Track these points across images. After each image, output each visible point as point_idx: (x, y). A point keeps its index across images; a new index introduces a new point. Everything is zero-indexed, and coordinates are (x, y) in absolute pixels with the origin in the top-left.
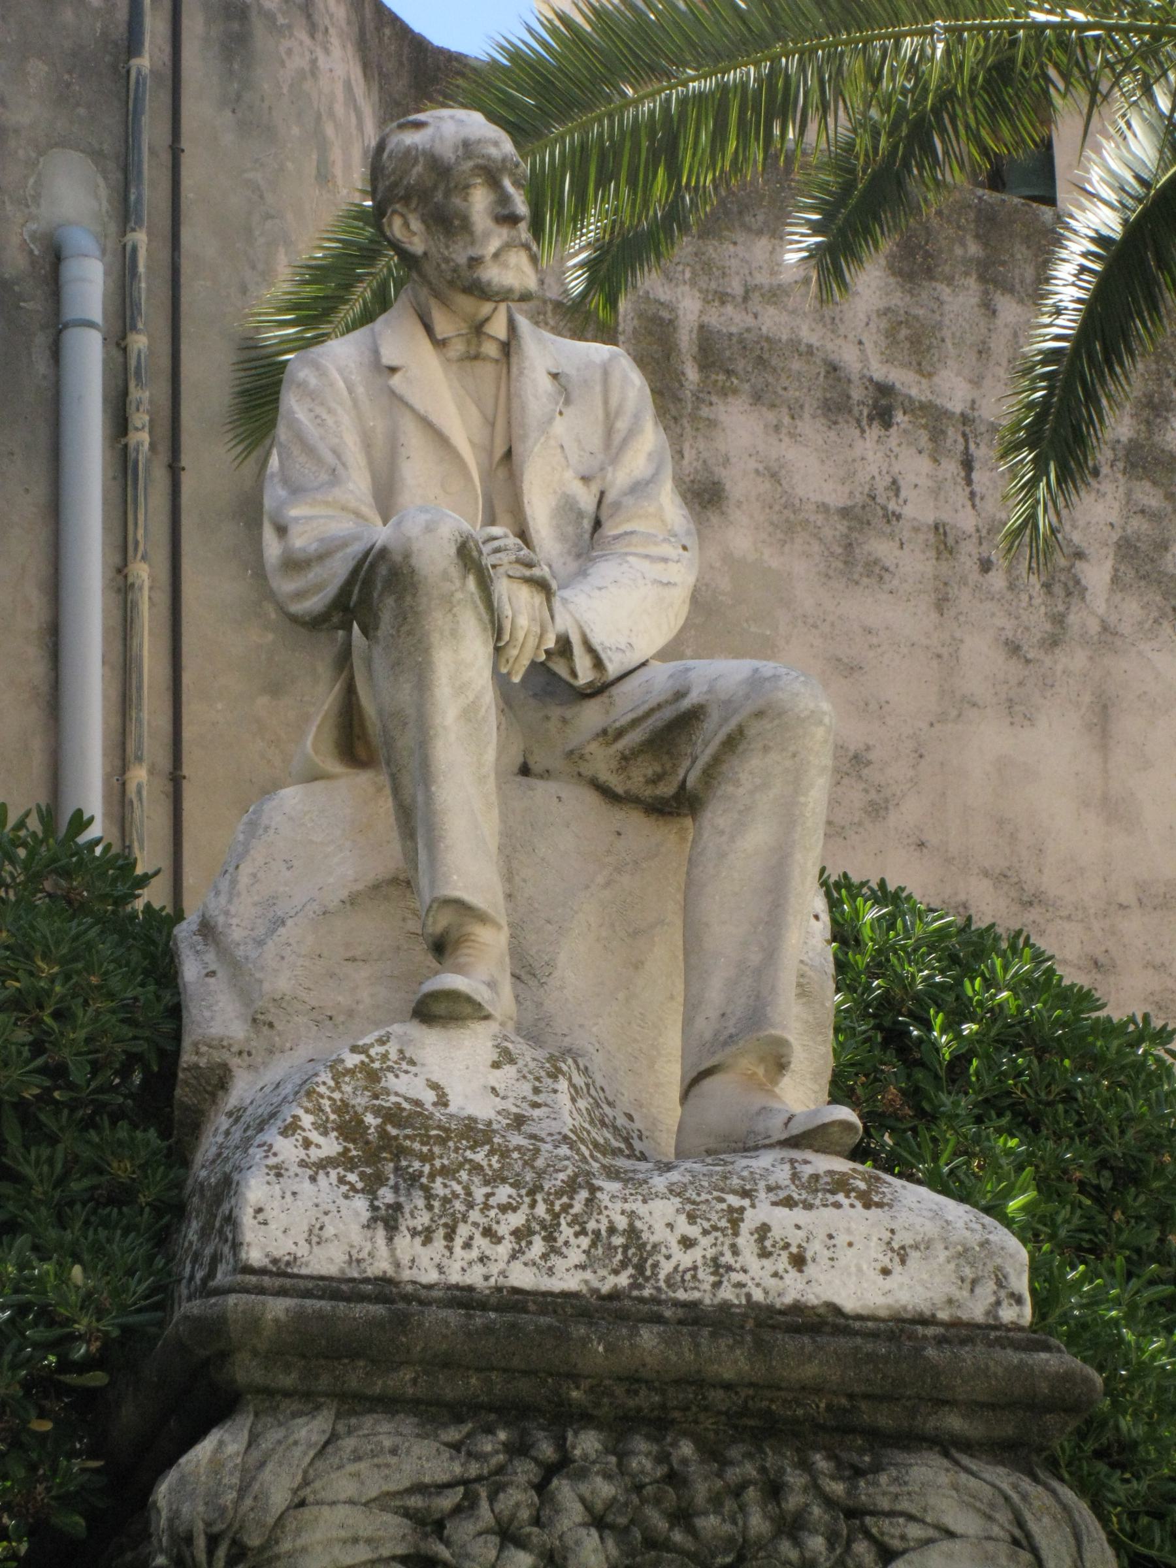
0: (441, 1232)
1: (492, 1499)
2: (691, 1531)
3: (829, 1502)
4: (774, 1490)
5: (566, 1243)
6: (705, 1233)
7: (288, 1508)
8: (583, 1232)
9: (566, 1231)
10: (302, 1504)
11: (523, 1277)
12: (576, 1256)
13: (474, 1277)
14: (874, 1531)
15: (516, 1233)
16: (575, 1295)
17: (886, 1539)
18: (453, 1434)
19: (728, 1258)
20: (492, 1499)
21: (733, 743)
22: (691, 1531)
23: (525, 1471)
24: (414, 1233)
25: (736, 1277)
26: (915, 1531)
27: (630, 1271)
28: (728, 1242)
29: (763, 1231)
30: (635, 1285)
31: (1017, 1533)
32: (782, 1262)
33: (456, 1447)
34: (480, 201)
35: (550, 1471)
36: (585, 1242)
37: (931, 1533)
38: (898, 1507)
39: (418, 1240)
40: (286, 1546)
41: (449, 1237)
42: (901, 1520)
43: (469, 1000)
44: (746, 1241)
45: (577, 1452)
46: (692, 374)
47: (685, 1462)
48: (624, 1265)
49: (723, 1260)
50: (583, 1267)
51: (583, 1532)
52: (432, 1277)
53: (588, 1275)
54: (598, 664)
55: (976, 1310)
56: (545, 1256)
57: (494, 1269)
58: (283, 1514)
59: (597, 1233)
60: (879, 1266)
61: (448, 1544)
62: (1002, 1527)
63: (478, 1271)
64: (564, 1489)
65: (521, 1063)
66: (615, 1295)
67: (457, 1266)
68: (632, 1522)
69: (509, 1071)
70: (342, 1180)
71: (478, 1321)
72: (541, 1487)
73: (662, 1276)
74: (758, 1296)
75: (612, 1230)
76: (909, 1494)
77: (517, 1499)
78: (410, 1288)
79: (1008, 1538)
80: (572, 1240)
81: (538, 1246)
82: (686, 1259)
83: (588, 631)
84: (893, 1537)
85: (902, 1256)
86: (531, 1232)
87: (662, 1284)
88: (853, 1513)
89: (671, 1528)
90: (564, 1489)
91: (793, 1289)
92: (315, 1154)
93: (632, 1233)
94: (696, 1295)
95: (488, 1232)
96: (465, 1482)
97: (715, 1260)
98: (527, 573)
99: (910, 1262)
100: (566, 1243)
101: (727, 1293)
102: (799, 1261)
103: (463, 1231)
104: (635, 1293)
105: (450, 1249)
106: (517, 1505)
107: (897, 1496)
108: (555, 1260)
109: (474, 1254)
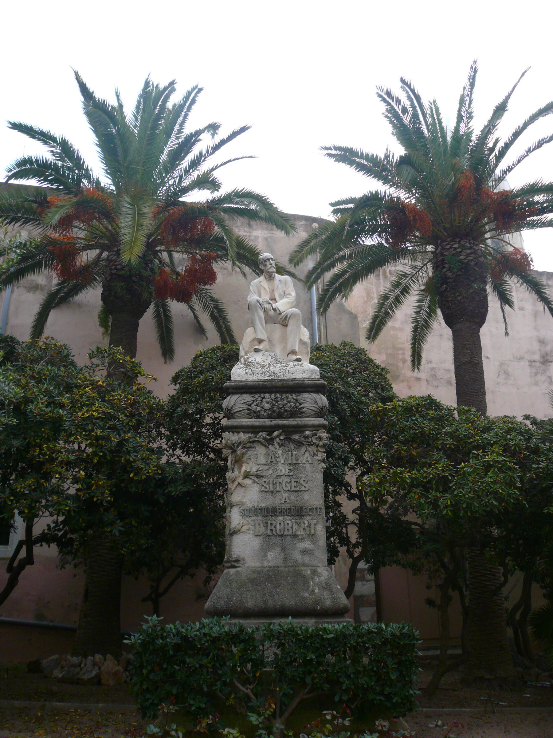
3: (294, 399)
4: (288, 398)
11: (261, 378)
13: (256, 379)
21: (289, 318)
23: (259, 399)
26: (303, 402)
32: (291, 374)
34: (268, 263)
44: (287, 372)
46: (389, 275)
64: (264, 400)
72: (261, 400)
90: (264, 400)
91: (293, 376)
93: (274, 373)
101: (284, 378)
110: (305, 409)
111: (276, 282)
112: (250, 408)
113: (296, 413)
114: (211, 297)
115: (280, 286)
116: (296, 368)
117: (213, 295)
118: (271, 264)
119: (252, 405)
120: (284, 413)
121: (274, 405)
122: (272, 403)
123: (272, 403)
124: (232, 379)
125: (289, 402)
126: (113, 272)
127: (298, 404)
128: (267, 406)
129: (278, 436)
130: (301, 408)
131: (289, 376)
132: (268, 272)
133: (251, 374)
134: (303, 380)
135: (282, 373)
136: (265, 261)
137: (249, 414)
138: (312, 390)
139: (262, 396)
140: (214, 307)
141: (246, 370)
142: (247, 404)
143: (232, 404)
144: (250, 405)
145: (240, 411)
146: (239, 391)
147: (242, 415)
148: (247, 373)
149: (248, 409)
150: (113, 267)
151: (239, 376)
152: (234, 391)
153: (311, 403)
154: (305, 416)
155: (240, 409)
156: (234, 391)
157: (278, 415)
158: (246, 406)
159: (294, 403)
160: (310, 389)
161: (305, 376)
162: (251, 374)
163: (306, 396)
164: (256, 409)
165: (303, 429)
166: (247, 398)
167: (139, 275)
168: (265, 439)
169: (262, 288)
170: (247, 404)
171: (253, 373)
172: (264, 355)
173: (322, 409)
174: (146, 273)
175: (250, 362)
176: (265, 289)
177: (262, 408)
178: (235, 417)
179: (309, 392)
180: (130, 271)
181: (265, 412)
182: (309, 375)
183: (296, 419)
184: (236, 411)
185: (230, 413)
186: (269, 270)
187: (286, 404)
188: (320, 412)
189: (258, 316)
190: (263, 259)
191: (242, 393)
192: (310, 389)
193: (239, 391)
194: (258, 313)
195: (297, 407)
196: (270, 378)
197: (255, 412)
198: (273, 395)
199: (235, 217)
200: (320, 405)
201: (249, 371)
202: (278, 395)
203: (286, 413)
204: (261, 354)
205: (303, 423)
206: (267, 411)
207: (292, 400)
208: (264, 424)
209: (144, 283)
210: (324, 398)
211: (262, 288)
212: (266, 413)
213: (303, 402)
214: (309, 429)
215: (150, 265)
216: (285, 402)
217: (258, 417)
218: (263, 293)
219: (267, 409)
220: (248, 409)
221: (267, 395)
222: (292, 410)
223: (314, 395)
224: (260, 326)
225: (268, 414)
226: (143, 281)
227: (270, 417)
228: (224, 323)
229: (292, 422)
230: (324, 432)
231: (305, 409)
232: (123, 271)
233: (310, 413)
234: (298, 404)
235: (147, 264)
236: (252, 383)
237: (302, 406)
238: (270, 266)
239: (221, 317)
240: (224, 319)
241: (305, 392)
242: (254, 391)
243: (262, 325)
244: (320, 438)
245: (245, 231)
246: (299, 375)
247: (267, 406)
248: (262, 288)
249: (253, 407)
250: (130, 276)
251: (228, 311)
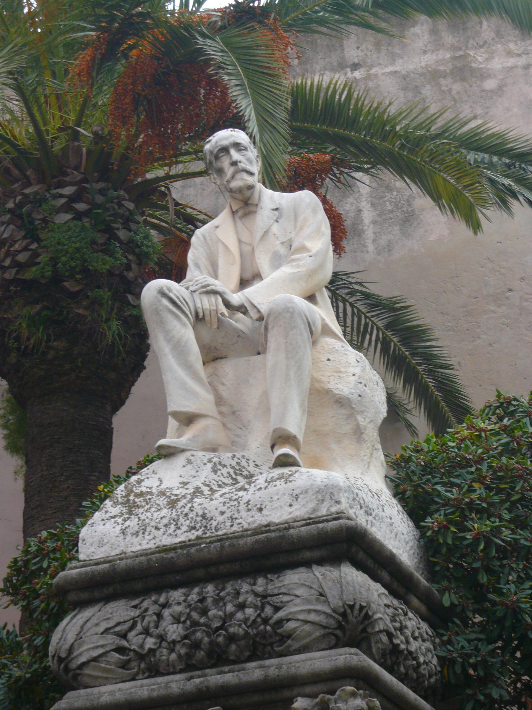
0: (142, 531)
1: (142, 622)
2: (208, 617)
3: (256, 595)
5: (182, 525)
6: (229, 508)
7: (76, 640)
8: (188, 519)
9: (182, 520)
10: (81, 638)
11: (167, 541)
12: (184, 528)
13: (152, 545)
14: (271, 602)
15: (166, 526)
16: (184, 542)
17: (276, 604)
18: (136, 602)
19: (236, 515)
20: (142, 622)
22: (208, 617)
24: (133, 534)
25: (238, 521)
26: (286, 598)
27: (203, 528)
28: (236, 509)
29: (248, 503)
30: (205, 533)
31: (321, 590)
32: (254, 512)
33: (135, 607)
35: (164, 606)
36: (188, 522)
37: (292, 598)
38: (281, 591)
39: (135, 536)
40: (75, 654)
41: (144, 533)
42: (280, 596)
43: (169, 447)
44: (243, 507)
45: (172, 599)
47: (208, 592)
48: (200, 527)
49: (234, 516)
50: (187, 531)
51: (171, 626)
52: (138, 548)
53: (189, 534)
54: (259, 311)
55: (323, 511)
56: (175, 531)
57: (157, 540)
58: (72, 645)
59: (192, 518)
60: (288, 504)
61: (128, 641)
62: (315, 590)
63: (153, 541)
64: (166, 613)
65: (194, 463)
66: (198, 538)
67: (145, 542)
68: (187, 619)
69: (190, 466)
70: (115, 522)
71: (137, 561)
73: (213, 528)
74: (246, 526)
75: (197, 515)
76: (284, 585)
77: (150, 619)
78: (132, 554)
79: (318, 594)
80: (184, 523)
81: (173, 527)
82: (220, 519)
83: (252, 300)
84: (277, 603)
85: (297, 497)
86: (170, 524)
87: (213, 531)
88: (264, 597)
89: (201, 617)
90: (166, 613)
91: (260, 519)
92: (108, 515)
93: (204, 516)
94: (224, 531)
95: (157, 528)
96: (133, 619)
97: (231, 517)
98: (204, 290)
99: (299, 500)
100: (182, 525)
101: (235, 528)
102: (260, 510)
103: (148, 529)
104: (204, 536)
105: (144, 537)
106: (149, 622)
107: (280, 587)
108: (179, 532)
109: (151, 537)
110: (291, 625)
111: (264, 216)
112: (124, 643)
113: (268, 640)
114: (367, 296)
115: (275, 228)
116: (271, 489)
117: (373, 289)
118: (234, 164)
119: (131, 635)
120: (228, 646)
121: (195, 624)
122: (189, 617)
123: (189, 617)
124: (82, 557)
125: (242, 607)
126: (7, 276)
127: (268, 610)
128: (174, 631)
130: (280, 623)
131: (249, 520)
132: (231, 191)
133: (137, 534)
134: (287, 526)
135: (228, 514)
136: (217, 157)
137: (124, 666)
138: (317, 554)
139: (162, 600)
140: (388, 327)
141: (125, 520)
142: (117, 634)
143: (71, 637)
144: (124, 636)
145: (95, 659)
146: (96, 594)
147: (105, 670)
148: (124, 532)
149: (120, 650)
150: (7, 262)
151: (101, 544)
152: (84, 596)
153: (308, 601)
154: (296, 646)
155: (95, 653)
156: (84, 596)
157: (210, 654)
158: (111, 640)
159: (256, 607)
160: (308, 555)
161: (300, 510)
162: (137, 534)
163: (293, 578)
164: (142, 646)
165: (286, 693)
166: (120, 611)
167: (85, 270)
169: (220, 247)
170: (117, 634)
171: (143, 529)
172: (189, 462)
173: (344, 615)
174: (102, 263)
175: (141, 494)
176: (226, 247)
177: (162, 638)
178: (86, 680)
179: (308, 564)
180: (54, 266)
181: (172, 650)
182: (311, 505)
183: (267, 662)
184: (83, 659)
185: (67, 669)
186: (234, 184)
187: (232, 615)
188: (340, 627)
189: (169, 339)
190: (211, 152)
191: (108, 599)
192: (308, 555)
193: (96, 594)
194: (167, 333)
195: (266, 621)
196: (193, 535)
197: (141, 657)
198: (196, 590)
199: (471, 15)
200: (335, 601)
201: (133, 523)
202: (210, 588)
203: (233, 647)
204: (181, 460)
205: (284, 671)
206: (178, 647)
207: (251, 599)
208: (163, 692)
209: (105, 294)
211: (221, 249)
212: (173, 656)
213: (286, 598)
214: (308, 689)
215: (122, 234)
216: (230, 608)
217: (154, 671)
219: (174, 642)
220: (120, 650)
221: (177, 595)
222: (251, 631)
223: (318, 571)
224: (180, 372)
225: (180, 656)
226: (99, 287)
227: (189, 666)
228: (431, 372)
229: (254, 672)
230: (354, 695)
231: (291, 625)
232: (34, 269)
233: (309, 634)
234: (268, 610)
235: (109, 231)
236: (129, 561)
237: (281, 614)
238: (232, 169)
239: (414, 355)
240: (429, 358)
241: (294, 566)
242: (139, 585)
243: (188, 367)
245: (509, 53)
247: (174, 631)
248: (221, 249)
249: (135, 640)
250: (57, 279)
251: (437, 333)
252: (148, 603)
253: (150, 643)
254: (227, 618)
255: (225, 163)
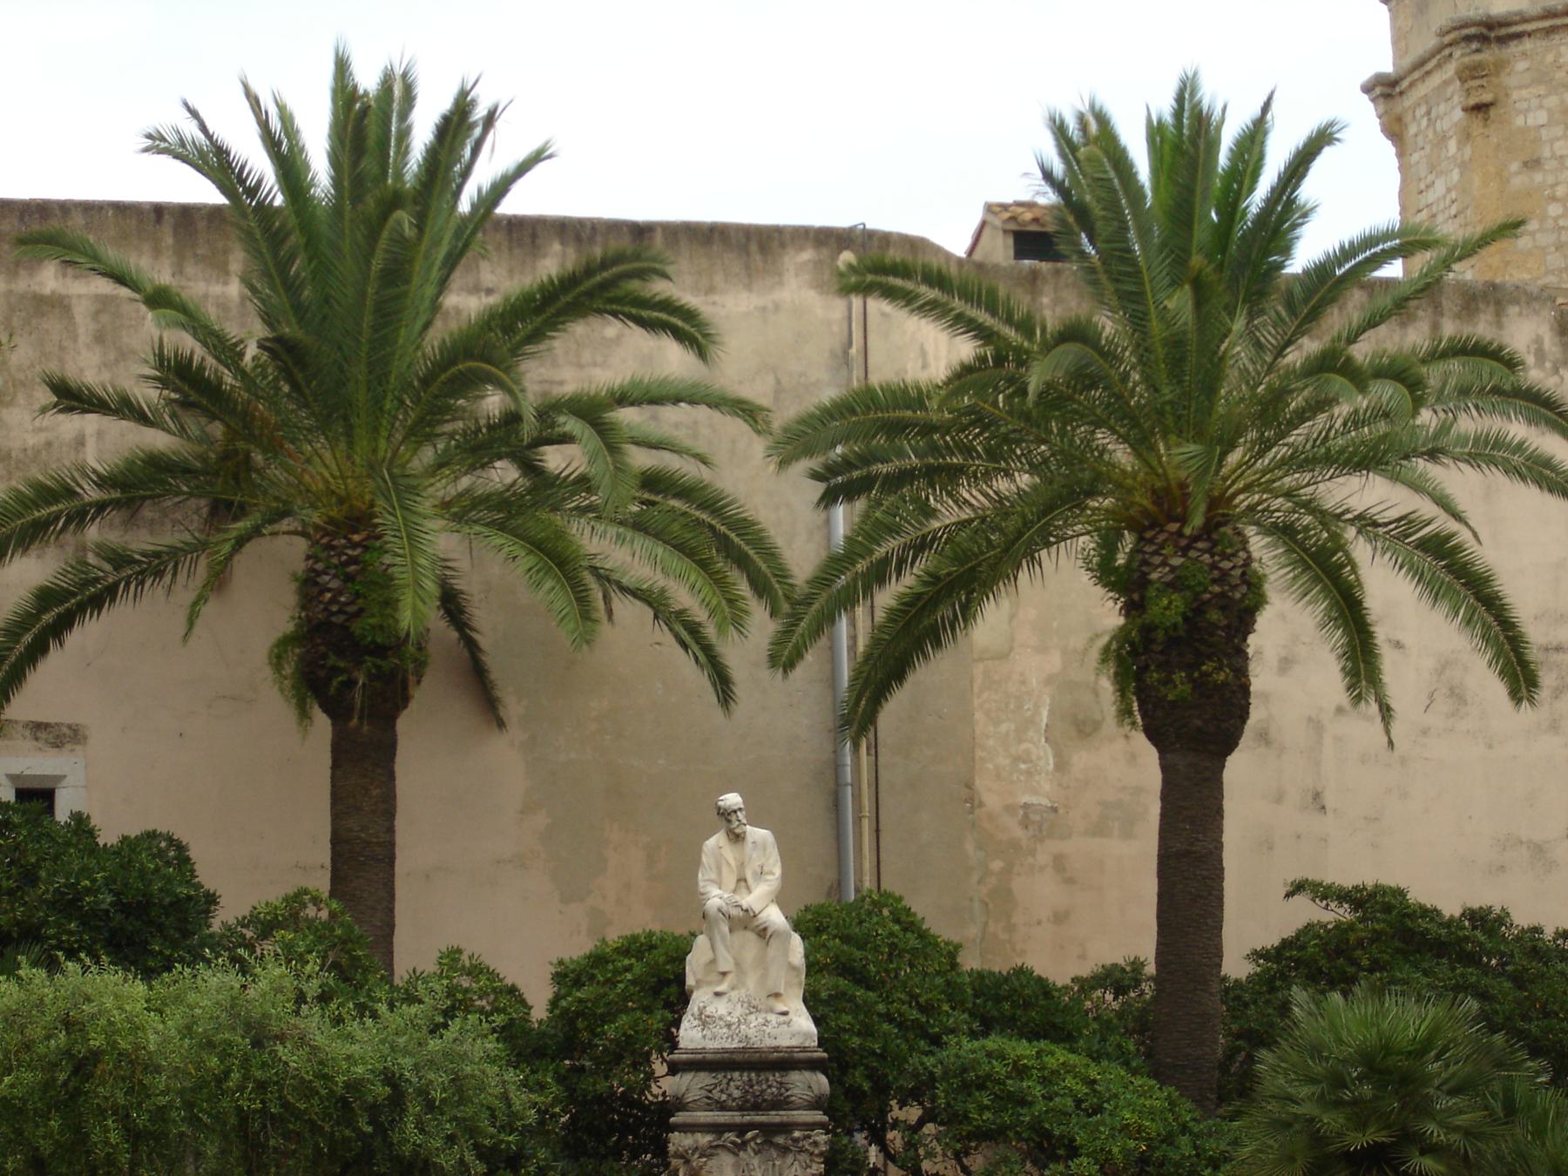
77: (724, 1086)
91: (775, 1043)
128: (737, 1093)
129: (753, 1139)
131: (769, 1043)
158: (704, 1093)
166: (704, 1079)
168: (733, 1143)
204: (725, 999)
210: (823, 1079)
218: (725, 869)
221: (736, 1075)
227: (740, 1109)
229: (775, 1117)
244: (816, 1144)
246: (785, 1042)
247: (737, 1093)
249: (716, 1094)
252: (720, 1076)
253: (724, 1097)
254: (763, 1091)
255: (733, 818)
